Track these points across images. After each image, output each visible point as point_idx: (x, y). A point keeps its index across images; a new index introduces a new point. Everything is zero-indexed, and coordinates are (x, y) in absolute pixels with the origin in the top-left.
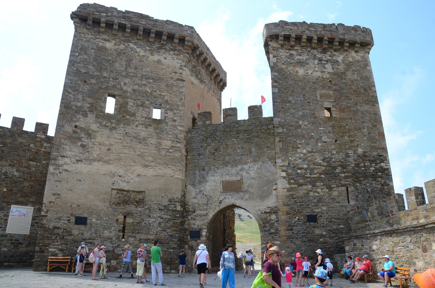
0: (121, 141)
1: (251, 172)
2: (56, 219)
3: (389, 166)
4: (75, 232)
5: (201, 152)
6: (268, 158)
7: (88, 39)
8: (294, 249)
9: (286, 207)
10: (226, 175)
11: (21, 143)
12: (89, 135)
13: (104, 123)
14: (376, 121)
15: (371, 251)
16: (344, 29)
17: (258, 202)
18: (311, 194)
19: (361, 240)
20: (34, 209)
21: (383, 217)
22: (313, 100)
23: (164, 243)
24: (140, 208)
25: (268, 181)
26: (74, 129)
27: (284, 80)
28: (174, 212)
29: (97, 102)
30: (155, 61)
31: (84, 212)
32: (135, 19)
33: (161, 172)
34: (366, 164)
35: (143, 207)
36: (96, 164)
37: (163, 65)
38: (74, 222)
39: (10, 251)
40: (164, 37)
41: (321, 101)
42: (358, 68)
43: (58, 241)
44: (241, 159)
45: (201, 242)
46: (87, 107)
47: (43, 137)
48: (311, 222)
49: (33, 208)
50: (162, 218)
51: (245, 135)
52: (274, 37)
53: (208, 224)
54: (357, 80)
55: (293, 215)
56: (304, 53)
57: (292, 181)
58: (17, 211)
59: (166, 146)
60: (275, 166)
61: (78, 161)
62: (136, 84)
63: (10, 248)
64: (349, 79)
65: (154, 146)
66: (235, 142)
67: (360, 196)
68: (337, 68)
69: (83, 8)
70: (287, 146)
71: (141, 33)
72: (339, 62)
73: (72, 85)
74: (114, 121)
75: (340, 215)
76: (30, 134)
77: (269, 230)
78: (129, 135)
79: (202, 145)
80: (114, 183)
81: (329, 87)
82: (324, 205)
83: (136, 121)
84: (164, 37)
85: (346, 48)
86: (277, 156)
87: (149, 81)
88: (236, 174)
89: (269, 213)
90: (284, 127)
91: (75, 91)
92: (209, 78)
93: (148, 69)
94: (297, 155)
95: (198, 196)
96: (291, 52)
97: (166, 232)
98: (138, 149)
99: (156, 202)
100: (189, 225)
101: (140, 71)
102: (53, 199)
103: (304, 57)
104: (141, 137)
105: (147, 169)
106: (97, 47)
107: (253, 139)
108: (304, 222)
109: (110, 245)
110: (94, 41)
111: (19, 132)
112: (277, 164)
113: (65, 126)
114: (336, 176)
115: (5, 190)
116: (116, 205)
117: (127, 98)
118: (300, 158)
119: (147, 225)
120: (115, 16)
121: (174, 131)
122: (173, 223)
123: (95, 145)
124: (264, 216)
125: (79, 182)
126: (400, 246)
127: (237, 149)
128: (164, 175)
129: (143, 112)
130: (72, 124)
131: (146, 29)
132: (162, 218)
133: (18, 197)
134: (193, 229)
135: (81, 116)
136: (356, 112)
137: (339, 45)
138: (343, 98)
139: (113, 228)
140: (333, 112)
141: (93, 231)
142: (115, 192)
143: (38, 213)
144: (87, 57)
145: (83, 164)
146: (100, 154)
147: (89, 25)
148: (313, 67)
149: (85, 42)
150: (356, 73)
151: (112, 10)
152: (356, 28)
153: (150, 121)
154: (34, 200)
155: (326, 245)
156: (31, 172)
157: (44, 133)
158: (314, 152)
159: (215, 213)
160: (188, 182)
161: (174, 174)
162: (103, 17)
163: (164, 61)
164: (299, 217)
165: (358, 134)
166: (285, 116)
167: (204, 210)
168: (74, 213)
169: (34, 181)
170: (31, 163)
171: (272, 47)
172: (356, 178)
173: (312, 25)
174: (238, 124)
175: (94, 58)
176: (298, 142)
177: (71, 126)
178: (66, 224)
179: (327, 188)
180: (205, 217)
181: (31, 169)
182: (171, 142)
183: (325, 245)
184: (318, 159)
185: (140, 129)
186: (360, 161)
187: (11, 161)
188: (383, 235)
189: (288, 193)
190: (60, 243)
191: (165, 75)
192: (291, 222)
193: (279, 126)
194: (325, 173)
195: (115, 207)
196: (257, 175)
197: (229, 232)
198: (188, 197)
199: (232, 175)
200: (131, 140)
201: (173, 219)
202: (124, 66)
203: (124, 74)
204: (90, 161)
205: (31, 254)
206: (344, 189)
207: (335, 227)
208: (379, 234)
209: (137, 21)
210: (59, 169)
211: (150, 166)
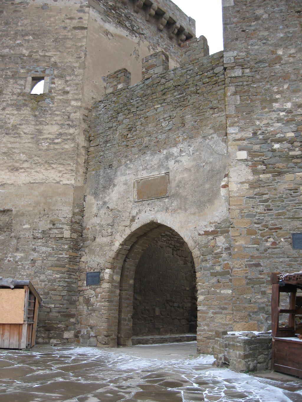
5: (109, 137)
6: (213, 127)
9: (246, 220)
17: (194, 214)
25: (213, 171)
30: (38, 8)
33: (39, 177)
44: (168, 137)
51: (175, 94)
53: (114, 258)
57: (260, 167)
60: (225, 141)
65: (30, 136)
66: (158, 110)
70: (252, 101)
79: (110, 125)
83: (4, 101)
87: (27, 38)
88: (159, 167)
90: (245, 66)
93: (26, 22)
94: (274, 116)
95: (101, 212)
99: (29, 227)
101: (15, 25)
104: (10, 126)
105: (16, 173)
112: (230, 137)
121: (65, 109)
122: (56, 259)
124: (204, 240)
127: (162, 122)
128: (43, 181)
129: (15, 86)
134: (91, 268)
159: (123, 240)
160: (88, 190)
161: (62, 179)
166: (248, 45)
182: (59, 127)
185: (8, 112)
189: (251, 191)
191: (53, 25)
198: (86, 215)
199: (153, 169)
211: (21, 168)
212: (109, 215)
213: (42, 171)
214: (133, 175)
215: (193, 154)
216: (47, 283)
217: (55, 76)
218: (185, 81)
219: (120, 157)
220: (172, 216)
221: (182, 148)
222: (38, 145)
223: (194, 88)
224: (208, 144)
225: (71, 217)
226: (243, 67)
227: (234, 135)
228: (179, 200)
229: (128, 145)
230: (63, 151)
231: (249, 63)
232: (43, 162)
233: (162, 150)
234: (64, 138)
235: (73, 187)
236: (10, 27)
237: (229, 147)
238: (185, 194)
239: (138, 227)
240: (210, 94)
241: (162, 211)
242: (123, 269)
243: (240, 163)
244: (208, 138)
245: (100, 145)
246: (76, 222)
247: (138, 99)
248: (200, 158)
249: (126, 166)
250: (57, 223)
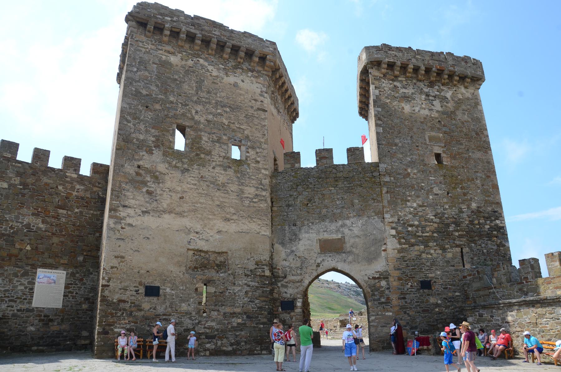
0: (196, 187)
2: (120, 289)
3: (505, 223)
4: (146, 306)
6: (374, 212)
7: (147, 50)
8: (408, 321)
9: (397, 272)
10: (324, 231)
11: (46, 184)
12: (157, 178)
13: (174, 163)
14: (489, 171)
15: (503, 323)
16: (454, 59)
17: (365, 265)
18: (424, 256)
19: (490, 310)
20: (67, 274)
21: (514, 284)
22: (422, 143)
23: (252, 318)
24: (221, 273)
26: (137, 169)
27: (389, 117)
28: (263, 278)
29: (164, 135)
30: (231, 84)
31: (156, 280)
32: (206, 28)
33: (245, 228)
34: (481, 221)
35: (225, 272)
36: (166, 216)
37: (240, 89)
38: (144, 293)
39: (39, 330)
40: (242, 54)
41: (431, 145)
42: (469, 107)
43: (124, 319)
45: (295, 314)
46: (152, 141)
47: (75, 176)
48: (425, 289)
49: (65, 272)
50: (249, 286)
51: (345, 183)
52: (376, 63)
54: (468, 121)
55: (406, 281)
56: (409, 85)
58: (45, 277)
59: (249, 194)
60: (382, 222)
61: (144, 212)
62: (210, 113)
63: (38, 327)
64: (459, 119)
65: (235, 194)
67: (475, 258)
68: (446, 106)
69: (143, 9)
70: (396, 198)
71: (214, 46)
72: (447, 99)
73: (131, 111)
74: (186, 160)
75: (455, 281)
76: (57, 172)
77: (379, 299)
78: (205, 179)
80: (190, 242)
81: (438, 128)
82: (437, 269)
83: (213, 161)
84: (242, 54)
85: (455, 82)
87: (225, 109)
89: (378, 278)
91: (135, 119)
92: (283, 107)
93: (223, 94)
94: (407, 210)
95: (290, 257)
96: (395, 83)
97: (254, 303)
98: (217, 197)
100: (279, 293)
101: (214, 95)
102: (115, 262)
103: (409, 91)
104: (220, 183)
105: (228, 223)
106: (159, 62)
107: (356, 188)
108: (418, 289)
109: (189, 321)
110: (155, 53)
111: (43, 168)
113: (126, 165)
114: (449, 235)
115: (28, 248)
116: (193, 270)
117: (200, 130)
118: (410, 213)
119: (232, 295)
120: (182, 22)
123: (164, 191)
124: (373, 282)
125: (147, 240)
126: (547, 318)
129: (220, 149)
130: (133, 163)
131: (220, 41)
132: (249, 286)
133: (46, 258)
135: (144, 153)
136: (468, 159)
137: (448, 78)
138: (454, 142)
139: (192, 300)
140: (443, 158)
141: (168, 304)
142: (192, 252)
143: (72, 279)
144: (148, 74)
145: (150, 217)
146: (172, 203)
147: (149, 31)
148: (420, 103)
149: (144, 53)
150: (466, 113)
151: (179, 14)
152: (466, 59)
153: (229, 161)
154: (66, 262)
155: (442, 316)
156: (61, 223)
157: (75, 170)
158: (425, 206)
160: (275, 240)
162: (167, 22)
163: (241, 84)
164: (411, 283)
165: (471, 186)
167: (298, 275)
168: (143, 281)
169: (65, 236)
170: (61, 211)
171: (374, 76)
172: (471, 238)
173: (419, 52)
175: (156, 75)
176: (408, 193)
177: (133, 166)
178: (133, 296)
179: (440, 249)
180: (299, 284)
181: (61, 220)
183: (440, 315)
184: (430, 215)
185: (218, 171)
186: (474, 218)
187: (35, 209)
188: (522, 305)
189: (399, 255)
190: (127, 322)
191: (243, 102)
192: (404, 289)
194: (438, 231)
195: (192, 273)
196: (362, 233)
198: (276, 259)
199: (331, 232)
200: (208, 186)
201: (261, 287)
202: (195, 88)
203: (195, 98)
204: (160, 212)
205: (65, 334)
206: (458, 250)
207: (450, 294)
208: (516, 304)
209: (210, 31)
210: (121, 223)
211: (232, 219)
212: (297, 260)
213: (248, 223)
216: (256, 309)
217: (249, 146)
222: (242, 201)
232: (247, 216)
236: (212, 96)
238: (357, 252)
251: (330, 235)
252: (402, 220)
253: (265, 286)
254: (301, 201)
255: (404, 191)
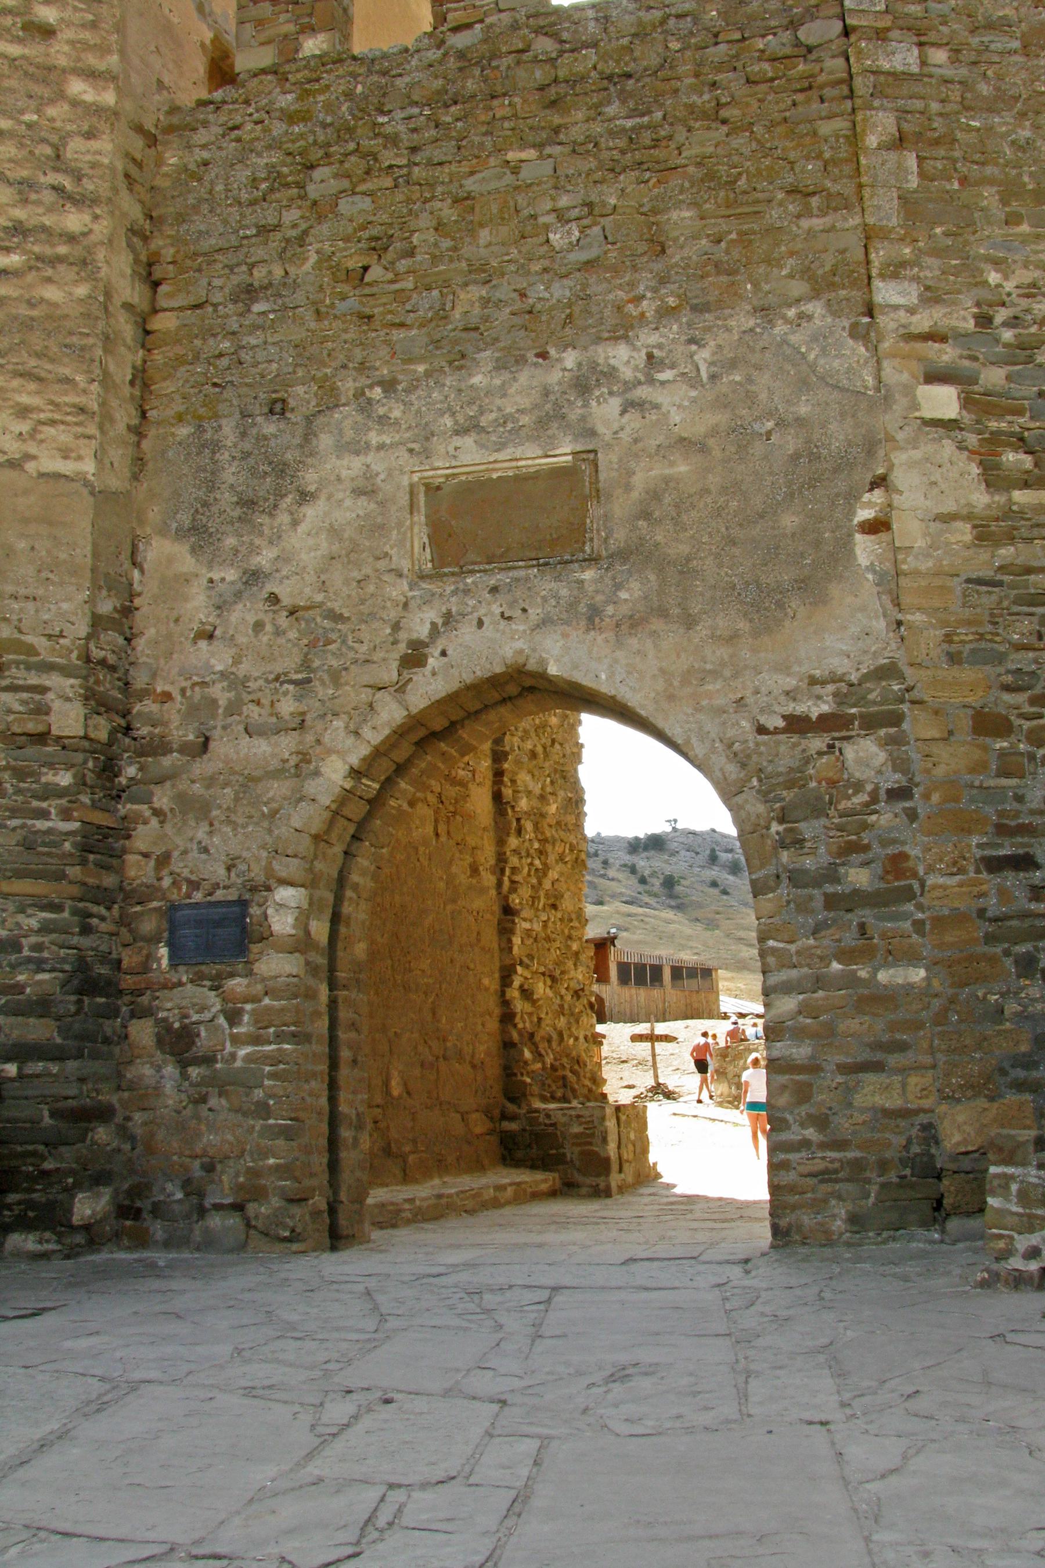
1: (661, 397)
5: (259, 273)
6: (806, 273)
9: (968, 674)
17: (732, 638)
51: (611, 110)
66: (525, 174)
70: (963, 181)
77: (831, 875)
86: (878, 257)
88: (542, 423)
89: (825, 723)
90: (932, 37)
107: (681, 134)
127: (547, 227)
134: (194, 885)
159: (365, 751)
160: (154, 514)
161: (32, 449)
174: (555, 36)
189: (984, 555)
192: (1019, 799)
193: (886, 22)
197: (537, 927)
212: (278, 632)
214: (407, 455)
215: (713, 377)
218: (654, 61)
219: (325, 366)
220: (619, 643)
221: (660, 346)
223: (706, 97)
224: (785, 342)
225: (83, 634)
226: (923, 39)
227: (902, 313)
228: (652, 577)
229: (373, 316)
230: (35, 313)
231: (944, 23)
233: (553, 352)
234: (37, 249)
235: (92, 494)
237: (885, 364)
238: (684, 549)
239: (443, 694)
240: (780, 129)
241: (567, 623)
242: (341, 881)
243: (934, 432)
244: (784, 317)
245: (215, 306)
246: (103, 662)
247: (416, 111)
248: (751, 398)
249: (362, 410)
250: (18, 663)
251: (500, 447)
252: (1005, 324)
253: (52, 806)
254: (324, 259)
255: (1025, 133)
